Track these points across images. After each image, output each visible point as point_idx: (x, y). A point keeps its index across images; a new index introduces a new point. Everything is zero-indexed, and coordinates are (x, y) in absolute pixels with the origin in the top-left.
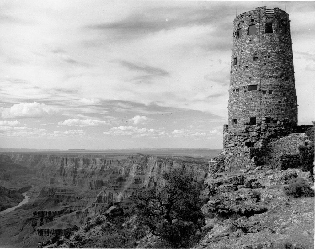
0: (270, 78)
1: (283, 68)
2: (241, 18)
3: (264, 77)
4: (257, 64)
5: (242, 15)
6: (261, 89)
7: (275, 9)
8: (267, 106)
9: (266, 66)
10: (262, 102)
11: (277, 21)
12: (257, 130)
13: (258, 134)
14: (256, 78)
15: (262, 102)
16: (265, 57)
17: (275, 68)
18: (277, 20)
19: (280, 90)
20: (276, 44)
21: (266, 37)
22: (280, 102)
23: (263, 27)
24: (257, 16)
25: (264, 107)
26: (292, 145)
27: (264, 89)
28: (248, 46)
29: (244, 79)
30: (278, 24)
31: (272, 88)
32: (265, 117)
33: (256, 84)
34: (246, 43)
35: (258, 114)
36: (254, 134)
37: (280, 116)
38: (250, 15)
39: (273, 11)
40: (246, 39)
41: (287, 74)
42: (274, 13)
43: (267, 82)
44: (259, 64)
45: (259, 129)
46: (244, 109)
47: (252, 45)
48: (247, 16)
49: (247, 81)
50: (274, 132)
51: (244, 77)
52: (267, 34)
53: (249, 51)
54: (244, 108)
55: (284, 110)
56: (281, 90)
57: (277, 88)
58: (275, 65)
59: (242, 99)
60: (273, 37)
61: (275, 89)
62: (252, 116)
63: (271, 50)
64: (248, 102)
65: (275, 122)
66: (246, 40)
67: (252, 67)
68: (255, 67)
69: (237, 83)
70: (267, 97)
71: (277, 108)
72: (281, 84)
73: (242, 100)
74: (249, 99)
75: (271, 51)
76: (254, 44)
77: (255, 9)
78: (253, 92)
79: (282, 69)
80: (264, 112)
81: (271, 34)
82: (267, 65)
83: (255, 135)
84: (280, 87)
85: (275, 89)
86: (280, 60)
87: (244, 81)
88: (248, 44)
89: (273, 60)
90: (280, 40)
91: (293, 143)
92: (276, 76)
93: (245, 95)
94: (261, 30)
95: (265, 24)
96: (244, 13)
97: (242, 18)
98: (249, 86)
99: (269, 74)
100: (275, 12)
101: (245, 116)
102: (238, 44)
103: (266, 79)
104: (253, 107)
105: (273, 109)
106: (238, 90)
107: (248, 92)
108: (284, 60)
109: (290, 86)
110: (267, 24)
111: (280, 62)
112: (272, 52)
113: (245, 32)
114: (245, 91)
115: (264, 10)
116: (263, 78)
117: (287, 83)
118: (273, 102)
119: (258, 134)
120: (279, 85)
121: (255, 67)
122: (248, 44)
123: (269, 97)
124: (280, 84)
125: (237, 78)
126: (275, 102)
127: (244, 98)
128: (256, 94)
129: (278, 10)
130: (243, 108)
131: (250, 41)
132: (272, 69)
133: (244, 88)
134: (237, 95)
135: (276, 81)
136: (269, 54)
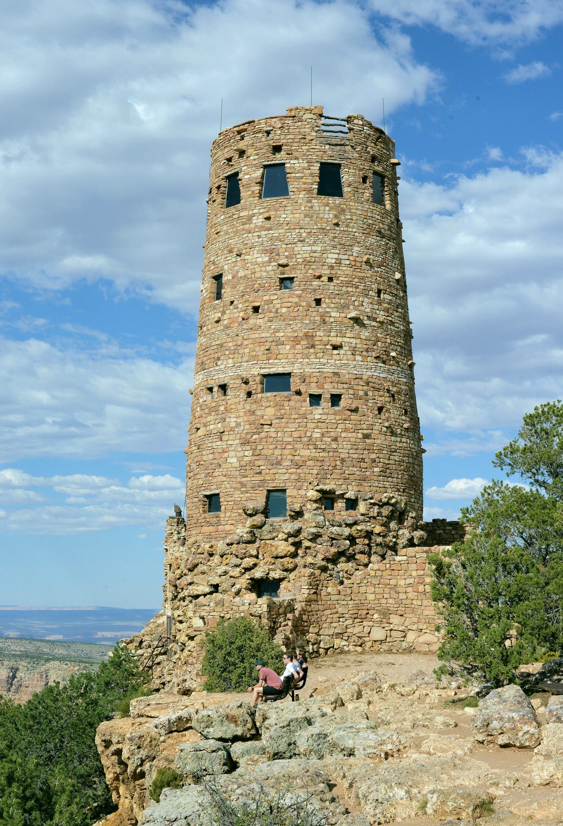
0: (335, 352)
1: (375, 320)
2: (238, 137)
3: (313, 346)
4: (291, 300)
5: (241, 127)
6: (303, 389)
7: (349, 120)
8: (324, 450)
9: (321, 310)
10: (309, 434)
12: (290, 535)
13: (292, 549)
14: (288, 347)
15: (309, 434)
16: (319, 277)
17: (350, 319)
18: (356, 155)
20: (354, 238)
21: (322, 208)
22: (366, 436)
23: (311, 175)
24: (292, 137)
25: (314, 453)
26: (410, 589)
27: (315, 391)
28: (259, 237)
29: (247, 351)
30: (361, 170)
31: (341, 386)
32: (318, 488)
33: (287, 370)
34: (252, 226)
35: (293, 477)
36: (279, 550)
37: (365, 484)
38: (268, 133)
39: (345, 126)
40: (255, 211)
42: (345, 130)
43: (324, 365)
44: (297, 300)
45: (299, 531)
46: (246, 459)
47: (275, 233)
48: (260, 135)
49: (255, 357)
50: (348, 542)
51: (246, 342)
52: (325, 199)
53: (265, 251)
54: (246, 453)
56: (370, 393)
57: (356, 387)
58: (351, 307)
59: (238, 421)
60: (343, 210)
62: (270, 485)
63: (336, 256)
64: (259, 433)
65: (352, 504)
66: (254, 215)
67: (274, 310)
68: (284, 310)
69: (219, 363)
70: (324, 417)
71: (356, 456)
72: (371, 374)
73: (238, 425)
74: (262, 422)
76: (281, 231)
77: (285, 113)
78: (278, 399)
79: (374, 324)
80: (315, 472)
81: (338, 200)
82: (324, 305)
83: (282, 554)
84: (368, 384)
85: (351, 392)
87: (245, 358)
88: (262, 228)
91: (411, 581)
92: (354, 345)
93: (248, 407)
94: (304, 183)
95: (319, 165)
96: (249, 123)
97: (242, 138)
98: (264, 376)
99: (330, 338)
100: (350, 129)
101: (249, 485)
102: (225, 228)
103: (321, 355)
104: (278, 452)
105: (343, 460)
106: (223, 388)
107: (259, 396)
108: (379, 292)
110: (324, 166)
111: (366, 300)
112: (339, 262)
113: (252, 189)
114: (249, 394)
115: (315, 117)
116: (312, 350)
118: (344, 435)
119: (292, 549)
120: (365, 377)
121: (284, 310)
122: (262, 228)
123: (330, 417)
124: (366, 374)
125: (221, 345)
126: (350, 435)
127: (246, 418)
128: (286, 403)
129: (361, 123)
130: (241, 454)
131: (268, 218)
132: (340, 319)
133: (246, 383)
134: (222, 408)
135: (354, 363)
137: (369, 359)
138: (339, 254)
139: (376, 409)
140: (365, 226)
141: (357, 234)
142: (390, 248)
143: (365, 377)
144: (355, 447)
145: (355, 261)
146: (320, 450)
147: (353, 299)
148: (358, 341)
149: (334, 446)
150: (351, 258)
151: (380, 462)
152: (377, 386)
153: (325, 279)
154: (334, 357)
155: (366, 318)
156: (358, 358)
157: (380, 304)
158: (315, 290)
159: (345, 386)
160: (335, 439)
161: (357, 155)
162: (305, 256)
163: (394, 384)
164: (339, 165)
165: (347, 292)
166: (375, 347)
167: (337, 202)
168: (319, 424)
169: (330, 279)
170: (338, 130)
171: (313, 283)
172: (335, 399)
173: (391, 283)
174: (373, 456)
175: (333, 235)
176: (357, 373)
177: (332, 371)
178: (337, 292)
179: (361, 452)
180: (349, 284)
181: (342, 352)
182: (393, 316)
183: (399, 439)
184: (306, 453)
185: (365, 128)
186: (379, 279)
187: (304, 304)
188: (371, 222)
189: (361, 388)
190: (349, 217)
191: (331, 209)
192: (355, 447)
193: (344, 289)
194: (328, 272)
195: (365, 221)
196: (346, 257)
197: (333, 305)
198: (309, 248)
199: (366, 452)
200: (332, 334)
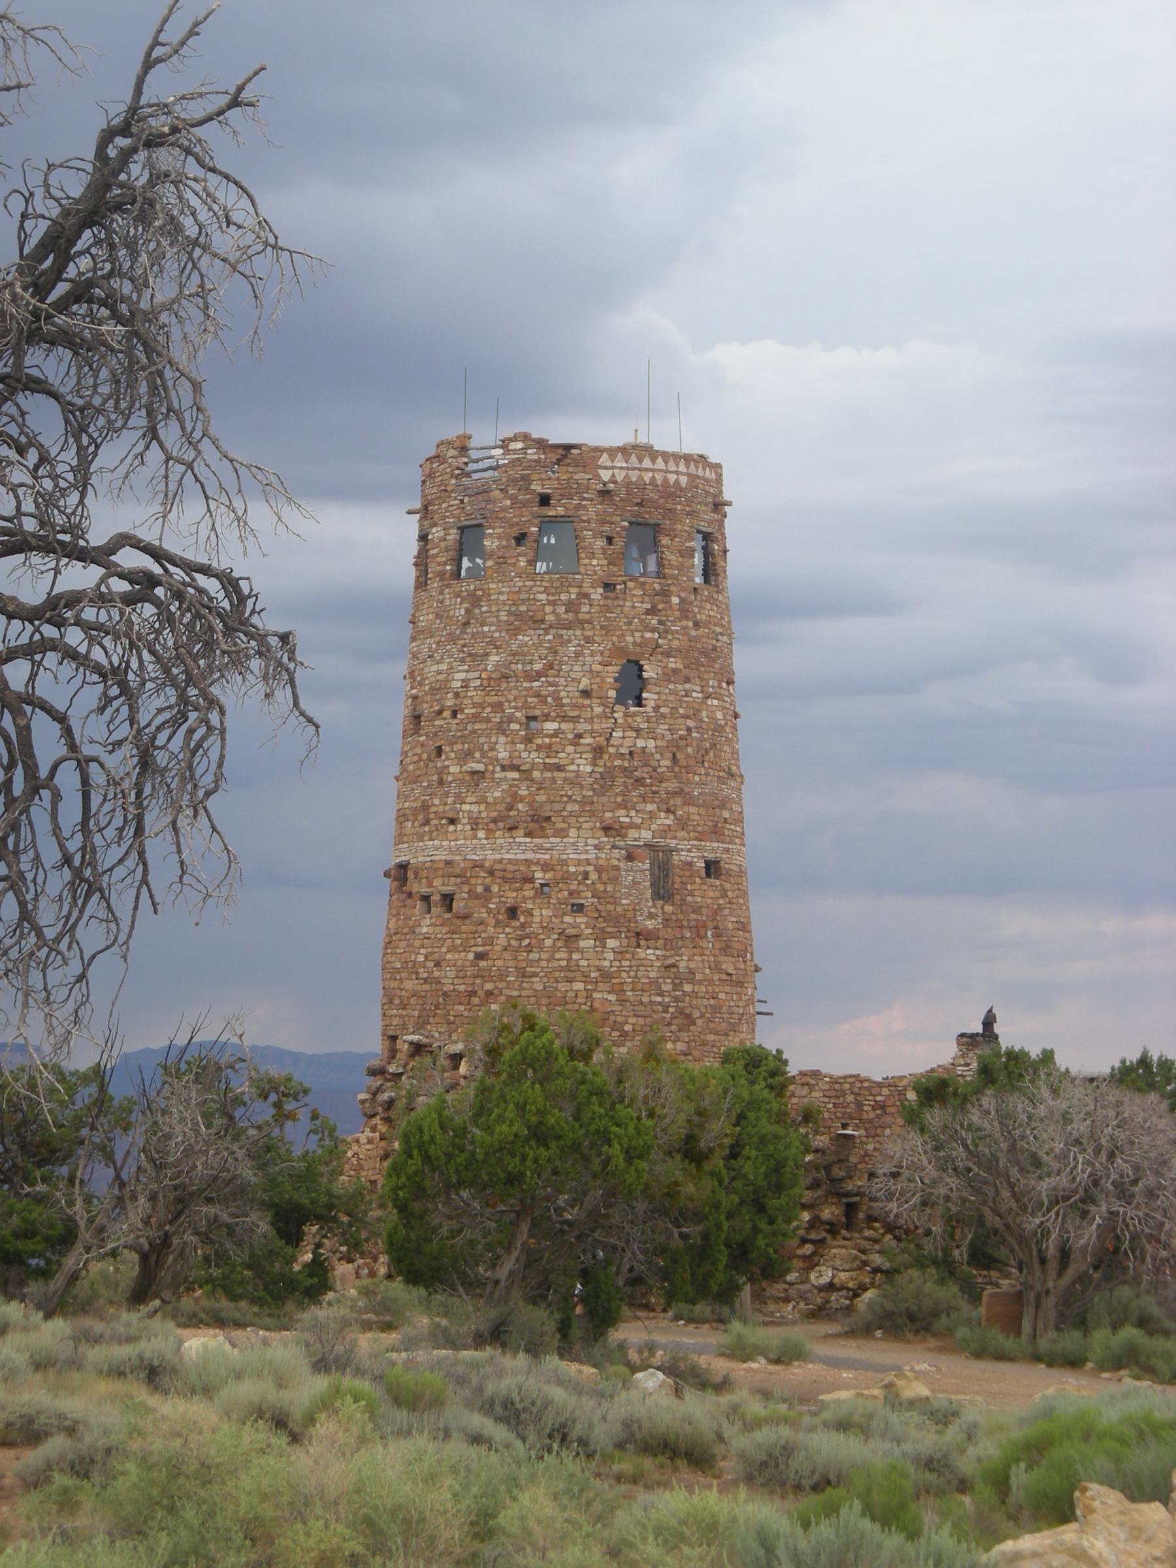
0: (451, 828)
3: (427, 822)
7: (504, 444)
8: (425, 980)
11: (503, 509)
16: (440, 712)
19: (487, 889)
20: (493, 643)
22: (480, 956)
41: (544, 798)
44: (418, 750)
55: (502, 999)
56: (495, 889)
57: (473, 881)
58: (477, 755)
60: (479, 599)
61: (466, 888)
63: (462, 676)
71: (462, 988)
72: (498, 857)
75: (463, 681)
82: (443, 757)
84: (491, 873)
85: (466, 888)
86: (501, 729)
89: (469, 727)
90: (510, 613)
92: (475, 815)
94: (439, 564)
109: (564, 863)
111: (502, 739)
112: (466, 683)
116: (427, 829)
117: (539, 848)
118: (449, 956)
120: (487, 864)
124: (491, 856)
126: (456, 956)
129: (520, 445)
135: (475, 842)
136: (457, 695)
137: (498, 833)
138: (467, 671)
139: (503, 911)
140: (512, 618)
141: (497, 635)
142: (569, 641)
143: (487, 864)
144: (461, 974)
145: (490, 679)
146: (421, 981)
147: (482, 740)
148: (483, 807)
149: (437, 974)
150: (484, 676)
151: (501, 994)
152: (510, 876)
153: (447, 714)
154: (451, 837)
155: (498, 769)
156: (481, 834)
157: (528, 740)
158: (435, 735)
159: (459, 880)
160: (437, 964)
161: (508, 502)
162: (432, 679)
163: (546, 867)
164: (480, 525)
165: (474, 732)
166: (511, 813)
167: (472, 587)
168: (426, 941)
169: (454, 714)
170: (487, 466)
171: (436, 723)
172: (448, 900)
173: (565, 701)
174: (489, 986)
175: (461, 642)
176: (476, 858)
177: (444, 858)
178: (459, 734)
179: (470, 981)
180: (476, 718)
181: (460, 827)
182: (560, 755)
183: (544, 956)
184: (408, 985)
185: (529, 451)
186: (529, 700)
187: (425, 756)
188: (523, 608)
189: (479, 882)
190: (485, 609)
191: (463, 599)
192: (461, 974)
193: (469, 727)
194: (449, 703)
195: (513, 609)
196: (477, 674)
197: (453, 755)
198: (434, 668)
199: (478, 981)
200: (450, 800)
